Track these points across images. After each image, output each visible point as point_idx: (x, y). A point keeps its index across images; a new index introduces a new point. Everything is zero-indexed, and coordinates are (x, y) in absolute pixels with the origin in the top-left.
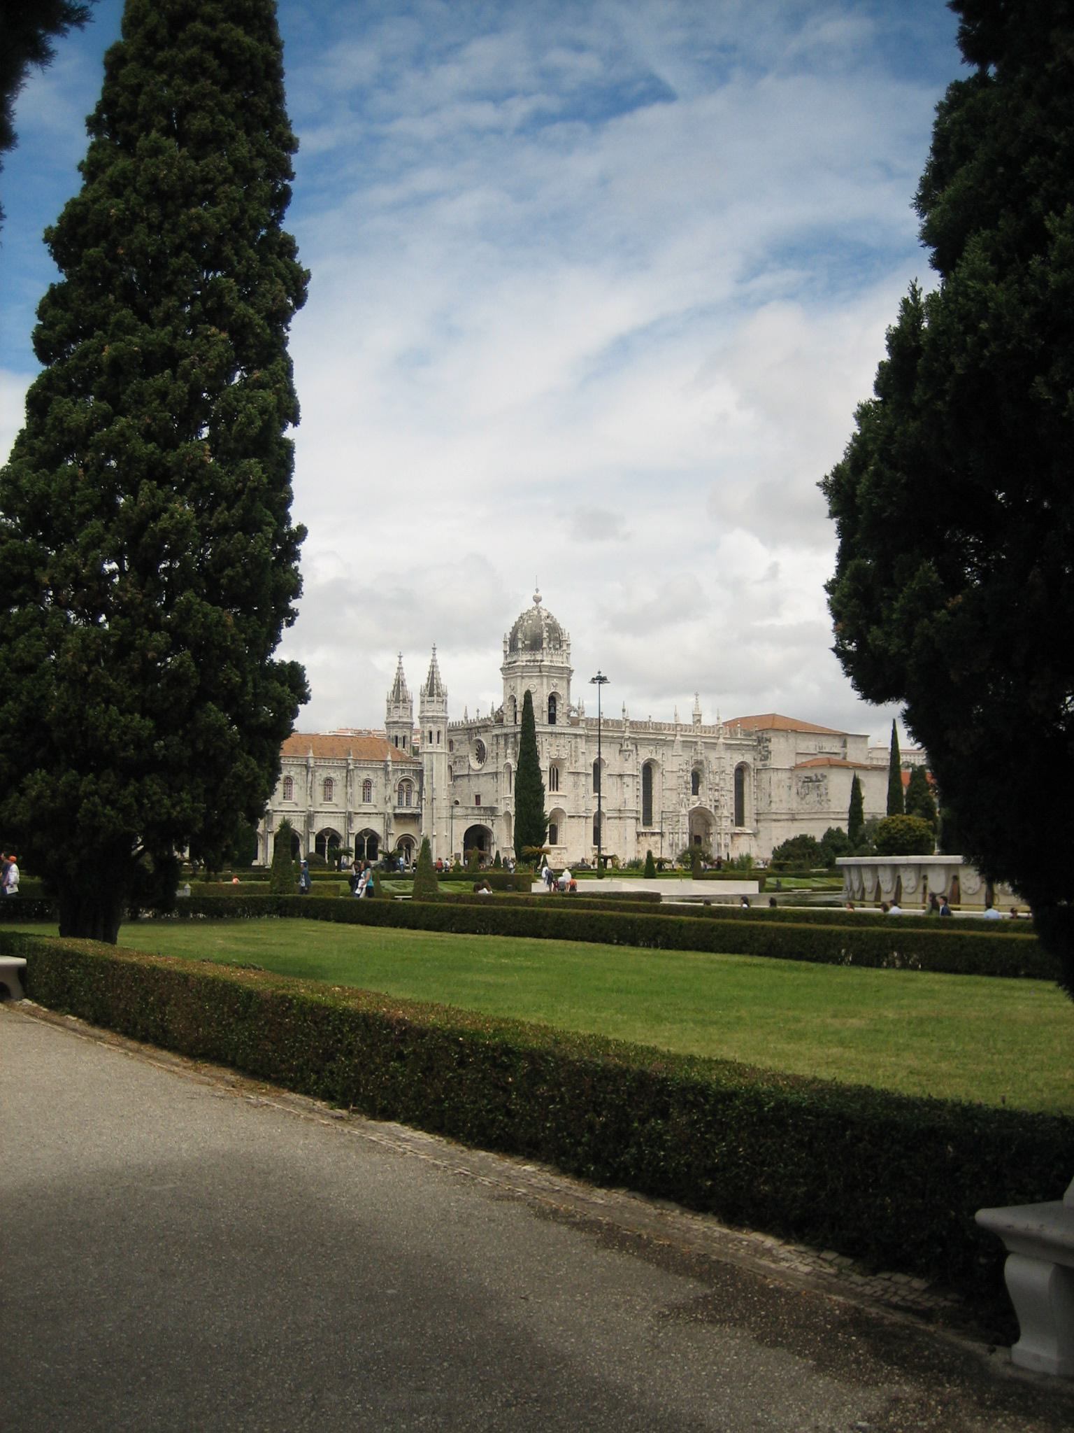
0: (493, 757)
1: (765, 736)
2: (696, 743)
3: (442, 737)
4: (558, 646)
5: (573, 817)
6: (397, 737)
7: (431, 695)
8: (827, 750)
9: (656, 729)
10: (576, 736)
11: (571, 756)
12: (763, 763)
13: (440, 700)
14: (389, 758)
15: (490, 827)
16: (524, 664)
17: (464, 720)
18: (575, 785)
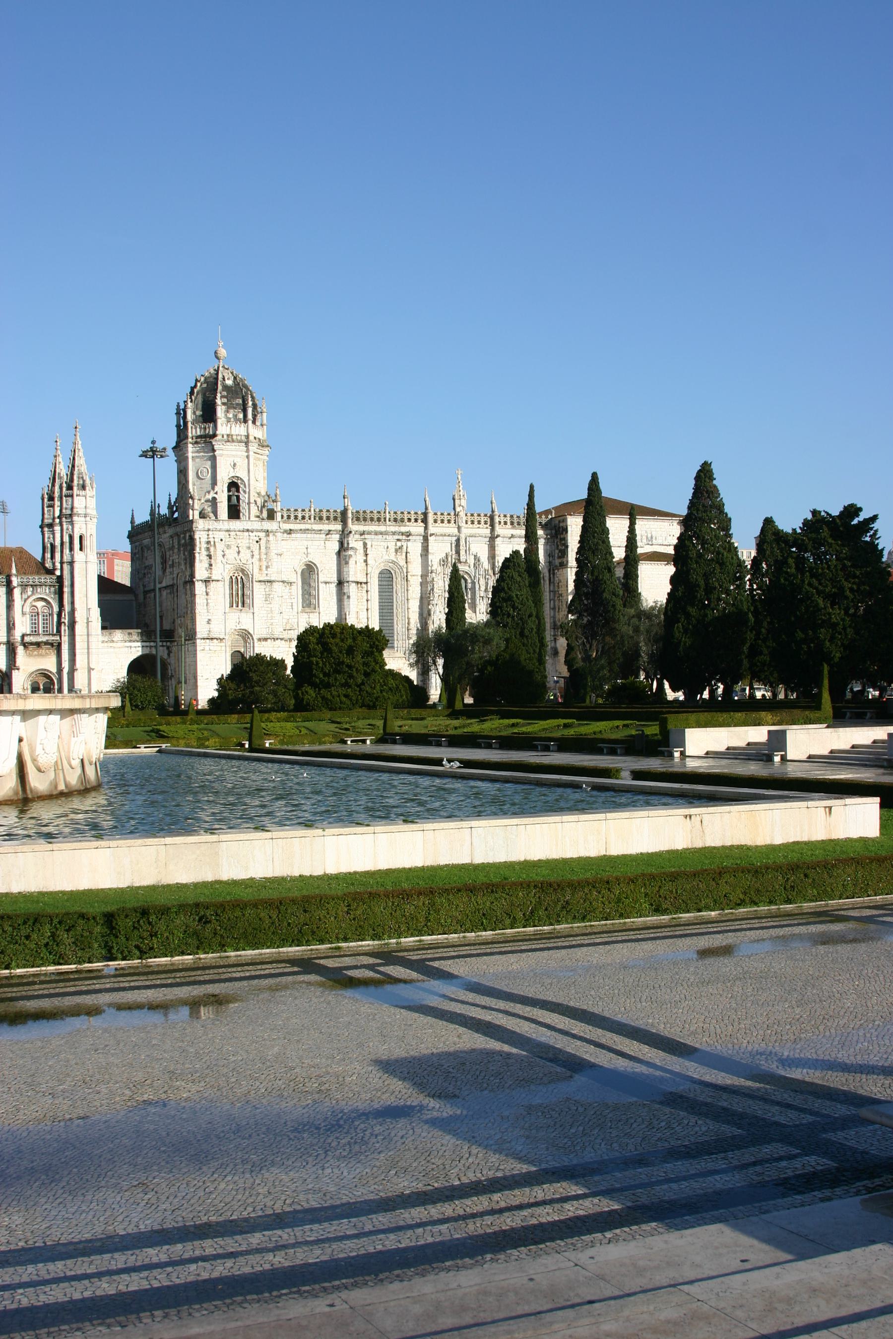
0: (170, 567)
1: (561, 525)
3: (86, 543)
4: (241, 416)
5: (266, 639)
7: (70, 487)
8: (660, 542)
9: (395, 520)
10: (267, 532)
11: (260, 560)
12: (560, 561)
13: (82, 493)
14: (14, 571)
15: (165, 657)
16: (195, 440)
17: (148, 518)
18: (267, 598)
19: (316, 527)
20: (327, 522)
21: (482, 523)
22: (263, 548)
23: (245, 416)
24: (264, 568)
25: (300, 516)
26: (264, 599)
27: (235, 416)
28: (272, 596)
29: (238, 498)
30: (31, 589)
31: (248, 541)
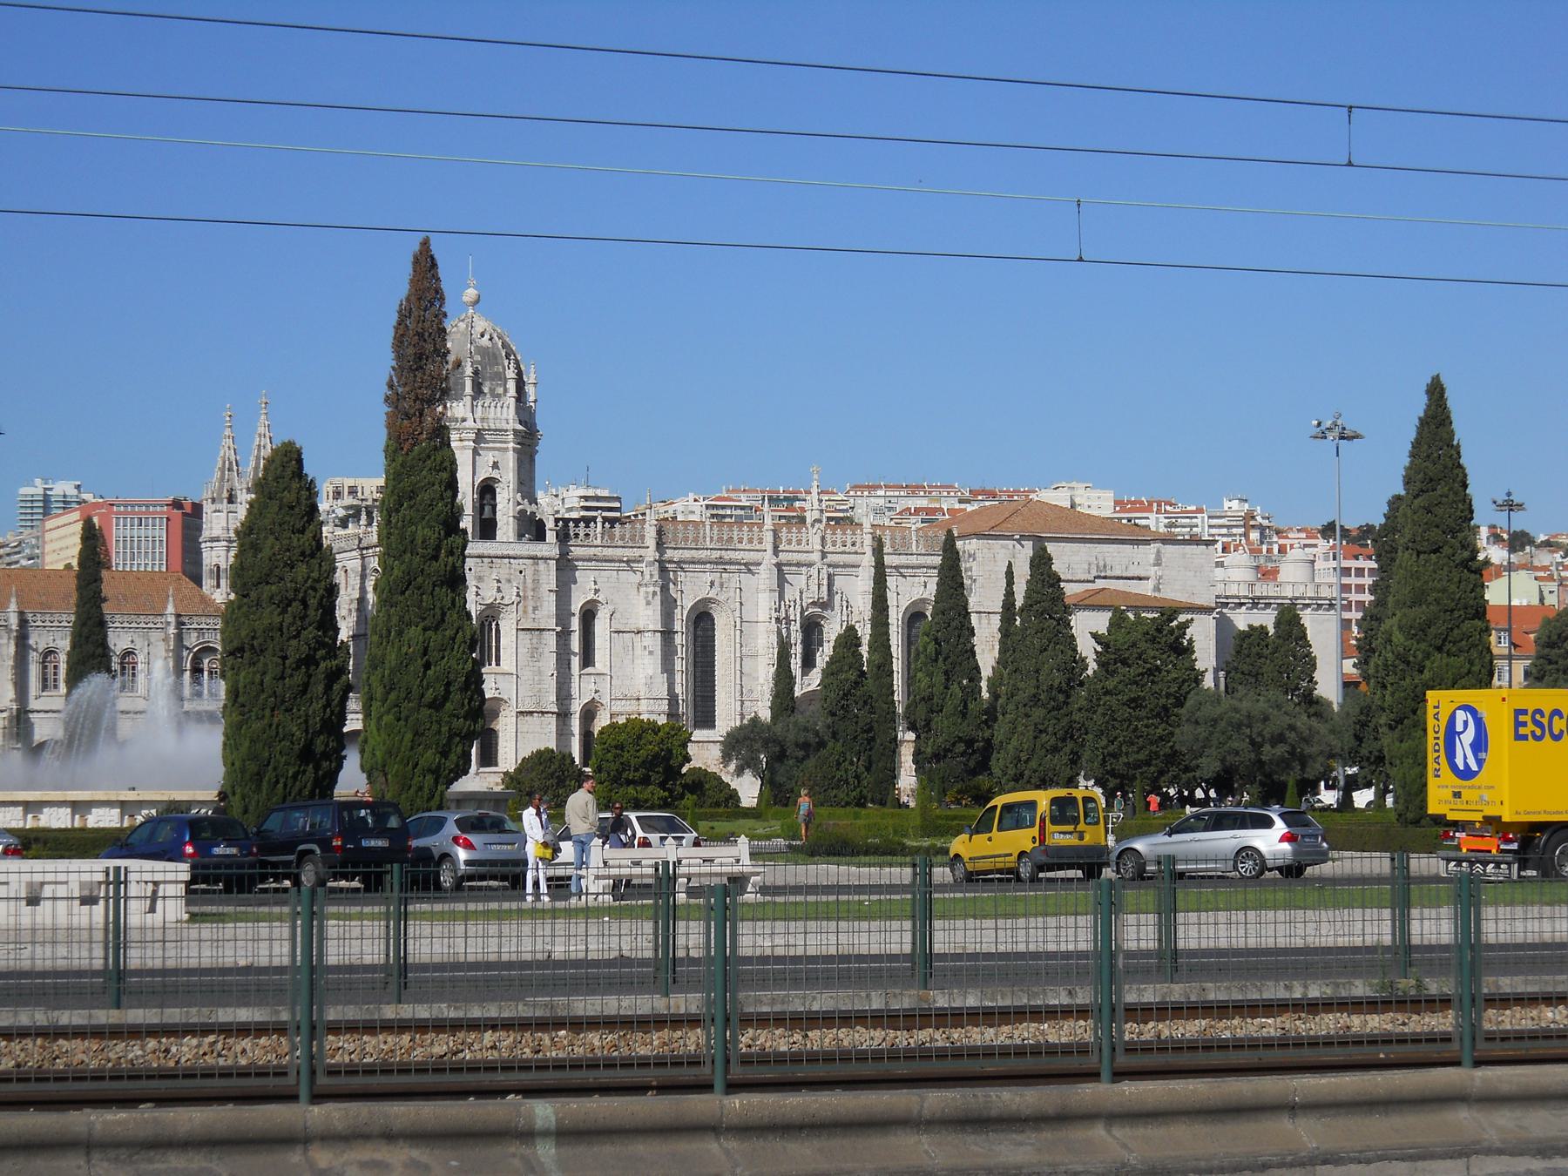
2: (810, 565)
4: (500, 390)
6: (218, 568)
8: (1117, 573)
14: (170, 609)
18: (535, 653)
19: (609, 552)
20: (620, 543)
21: (849, 544)
22: (529, 581)
23: (506, 390)
24: (530, 609)
25: (582, 534)
26: (529, 655)
27: (492, 390)
28: (540, 650)
29: (494, 507)
30: (196, 634)
31: (507, 571)
